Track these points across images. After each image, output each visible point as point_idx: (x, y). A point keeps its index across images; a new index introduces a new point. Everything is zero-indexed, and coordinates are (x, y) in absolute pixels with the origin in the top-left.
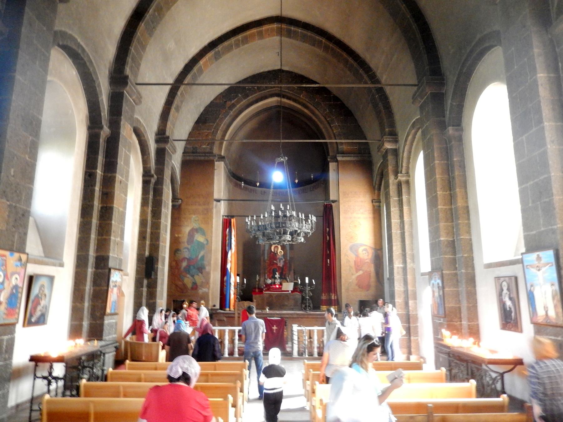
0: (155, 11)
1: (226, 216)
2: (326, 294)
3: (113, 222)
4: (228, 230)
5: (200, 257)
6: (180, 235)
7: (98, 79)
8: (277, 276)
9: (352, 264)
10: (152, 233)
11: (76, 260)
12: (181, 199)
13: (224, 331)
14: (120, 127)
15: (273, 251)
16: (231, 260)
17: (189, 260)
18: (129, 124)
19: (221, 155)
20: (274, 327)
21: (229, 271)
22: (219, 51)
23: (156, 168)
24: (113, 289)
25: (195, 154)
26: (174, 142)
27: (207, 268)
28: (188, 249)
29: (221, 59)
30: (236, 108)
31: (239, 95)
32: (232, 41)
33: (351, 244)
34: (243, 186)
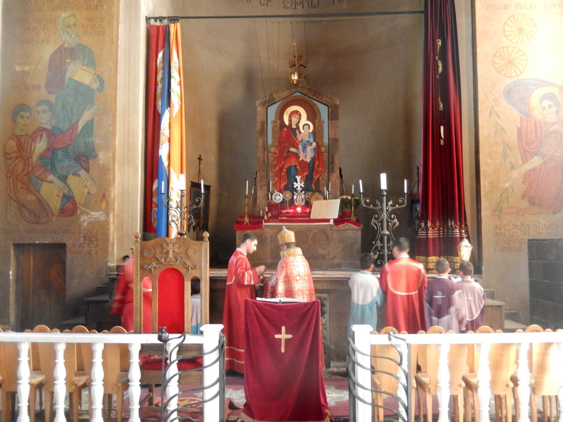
1: (156, 19)
2: (438, 224)
4: (160, 55)
5: (81, 125)
6: (27, 68)
8: (299, 184)
9: (513, 137)
13: (89, 347)
15: (287, 123)
16: (170, 136)
17: (51, 134)
20: (280, 333)
21: (166, 163)
27: (102, 155)
28: (49, 103)
33: (508, 81)
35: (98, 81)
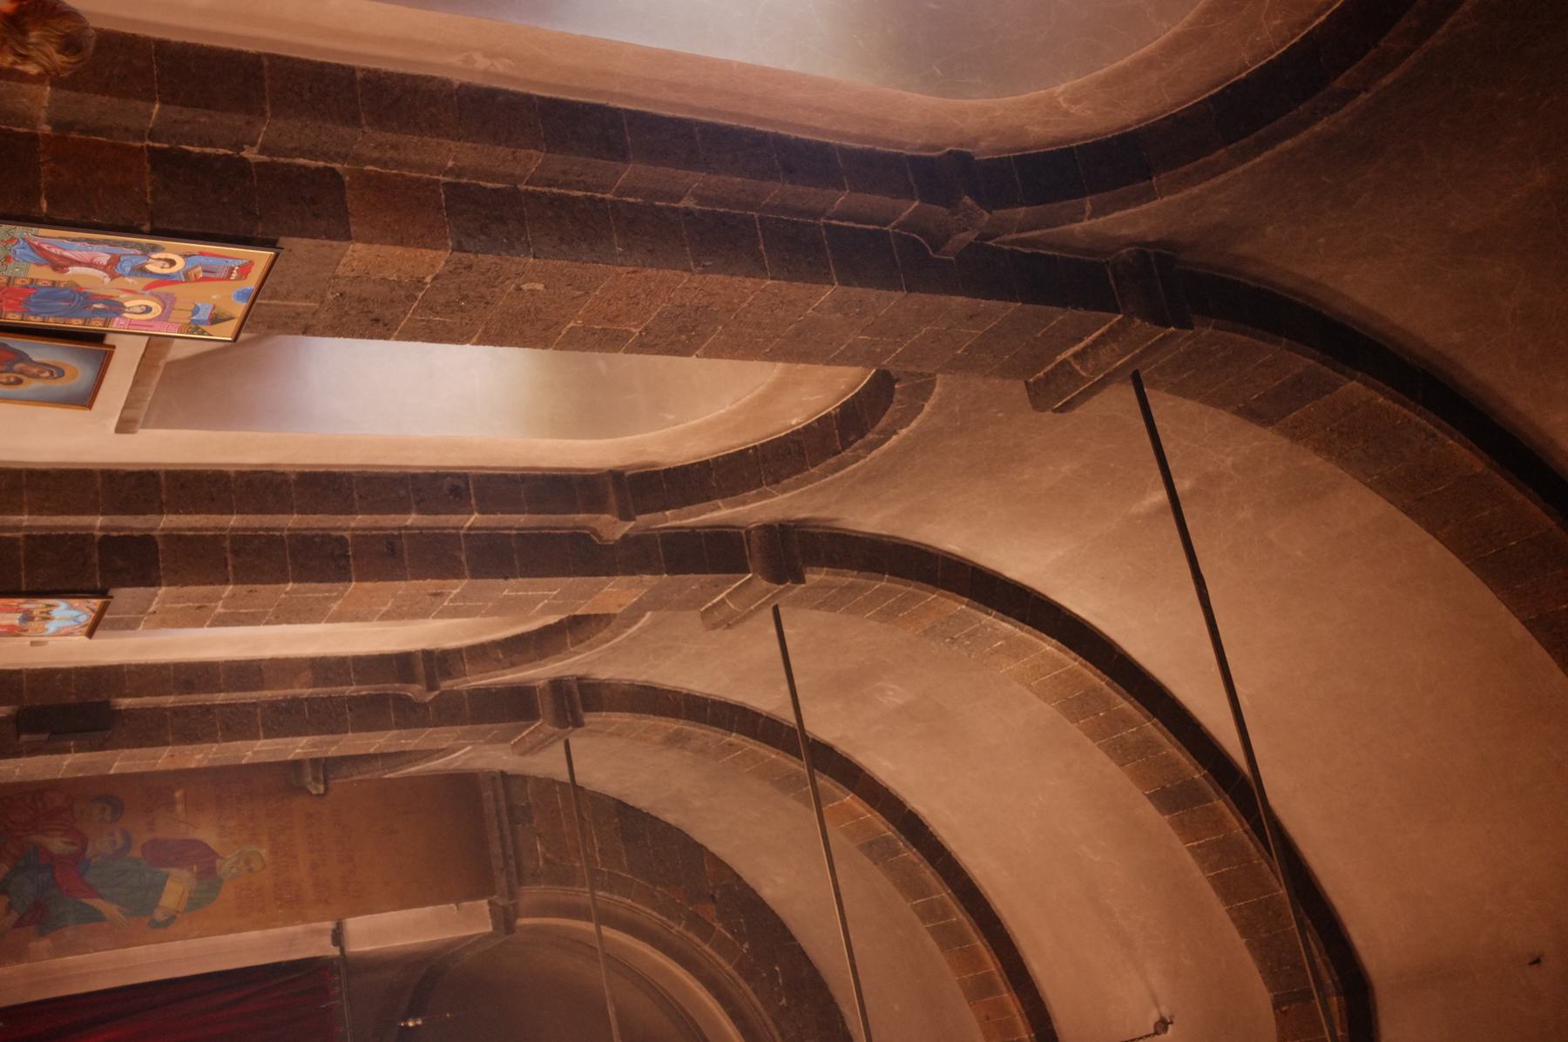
0: (1007, 637)
3: (290, 586)
5: (96, 903)
6: (179, 807)
7: (784, 491)
10: (207, 710)
11: (136, 469)
12: (326, 789)
14: (633, 574)
18: (640, 599)
19: (517, 916)
22: (897, 852)
23: (459, 693)
24: (17, 610)
25: (505, 818)
26: (560, 747)
27: (45, 943)
29: (867, 861)
30: (697, 940)
31: (746, 946)
32: (939, 894)
34: (407, 1027)
35: (166, 918)
